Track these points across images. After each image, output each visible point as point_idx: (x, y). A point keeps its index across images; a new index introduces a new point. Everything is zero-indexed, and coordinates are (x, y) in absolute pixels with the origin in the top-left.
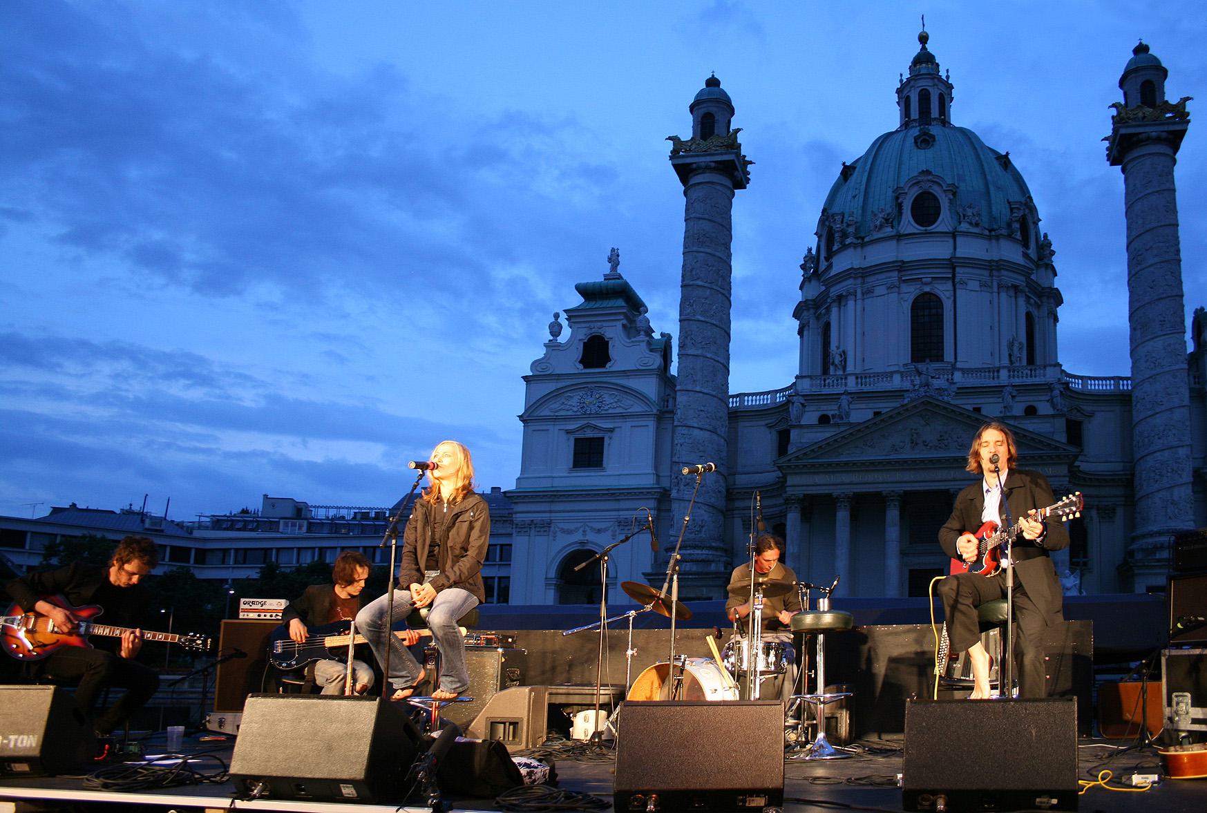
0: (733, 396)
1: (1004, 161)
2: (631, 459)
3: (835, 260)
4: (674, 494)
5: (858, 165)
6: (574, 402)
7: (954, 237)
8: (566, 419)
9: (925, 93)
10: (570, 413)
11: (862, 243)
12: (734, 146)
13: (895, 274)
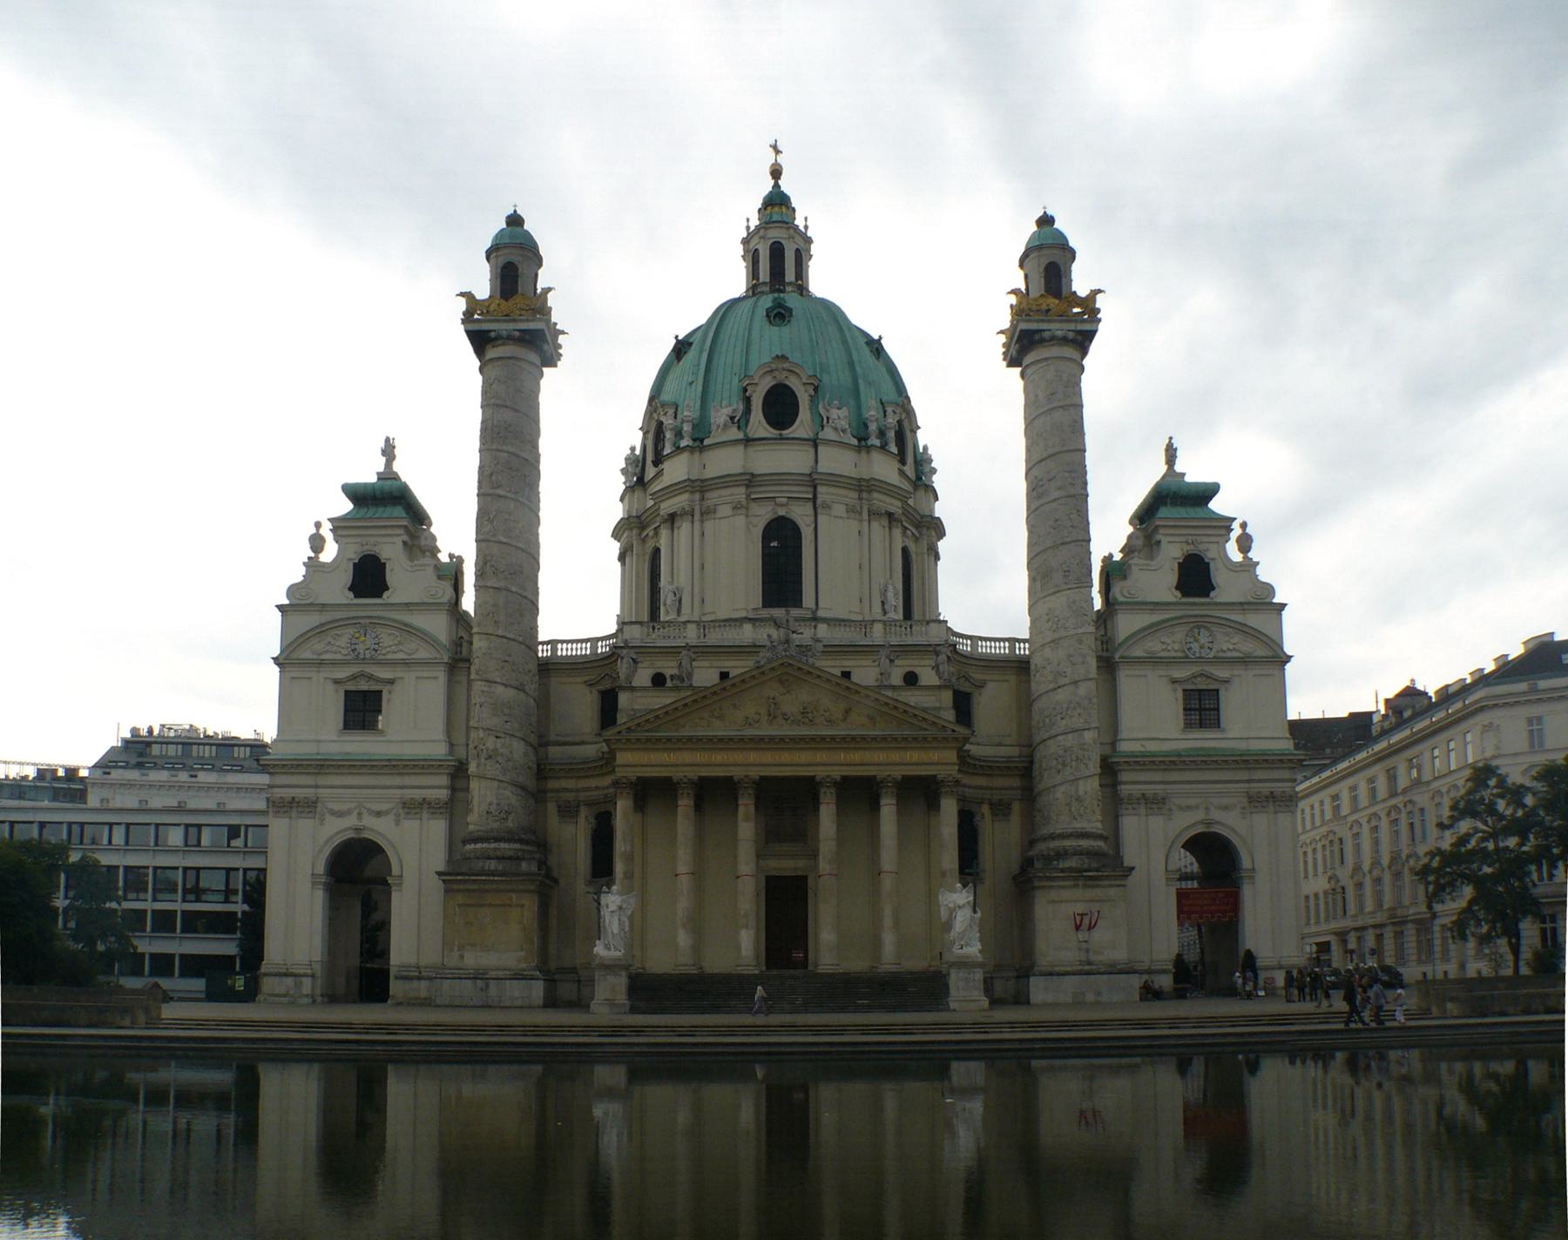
0: (543, 643)
1: (876, 347)
2: (416, 720)
3: (666, 466)
4: (472, 768)
5: (696, 339)
6: (343, 642)
7: (816, 446)
8: (334, 663)
9: (777, 249)
10: (338, 656)
11: (700, 443)
12: (545, 312)
13: (742, 490)
